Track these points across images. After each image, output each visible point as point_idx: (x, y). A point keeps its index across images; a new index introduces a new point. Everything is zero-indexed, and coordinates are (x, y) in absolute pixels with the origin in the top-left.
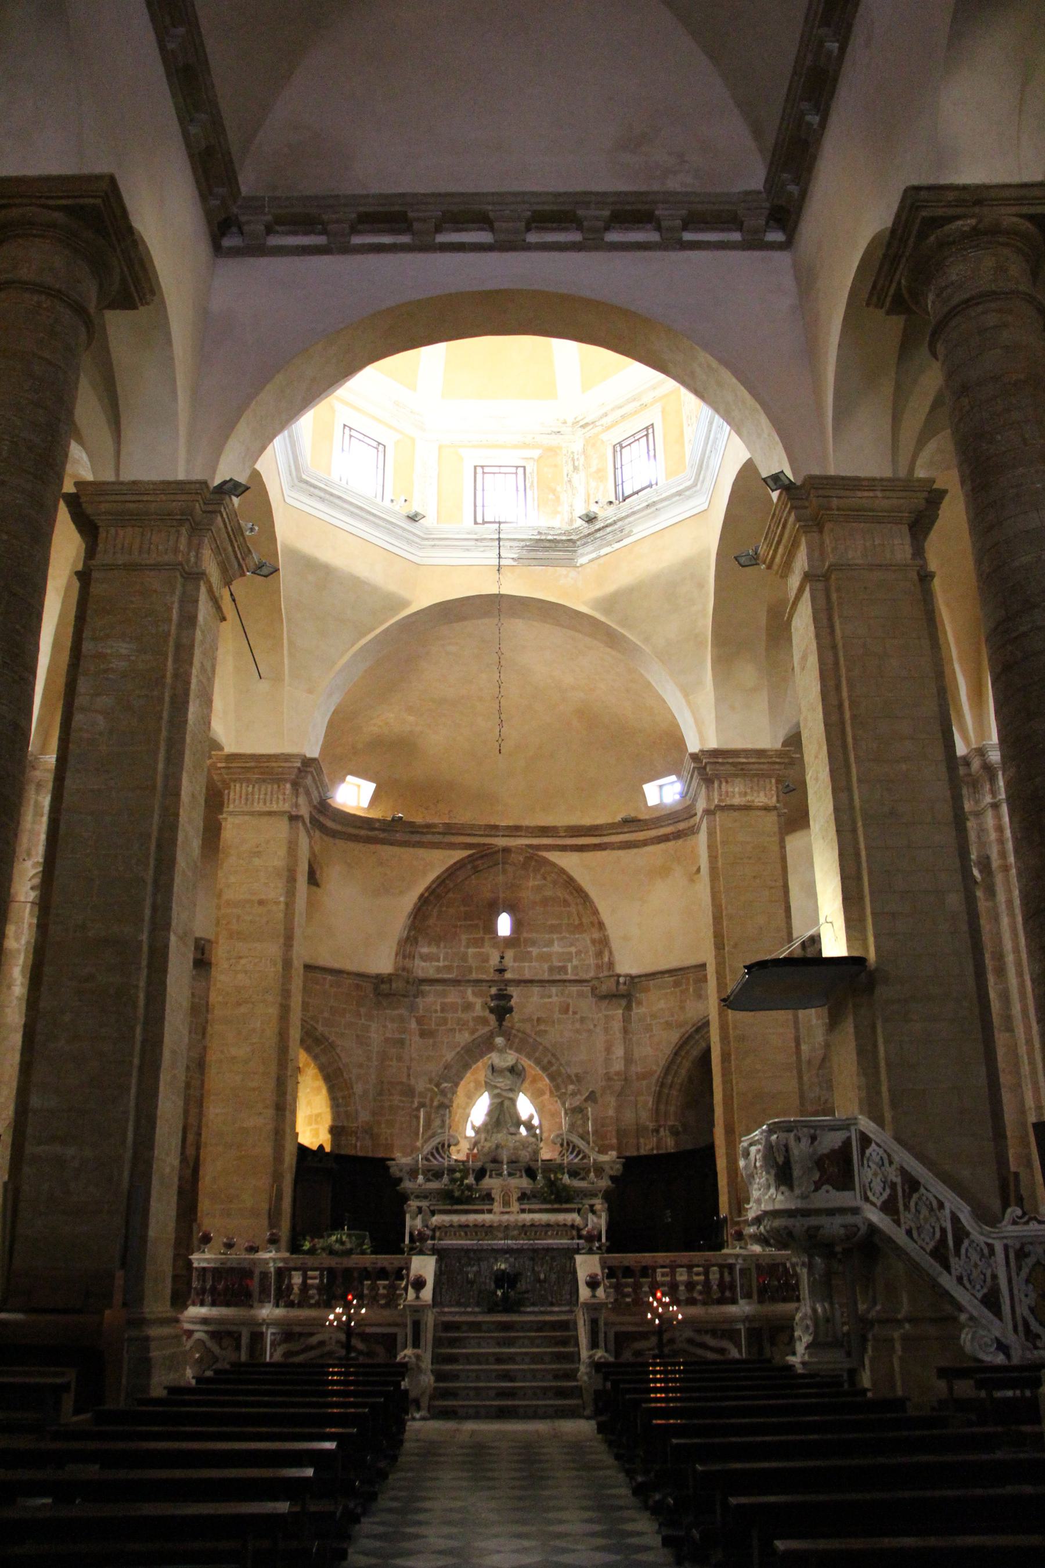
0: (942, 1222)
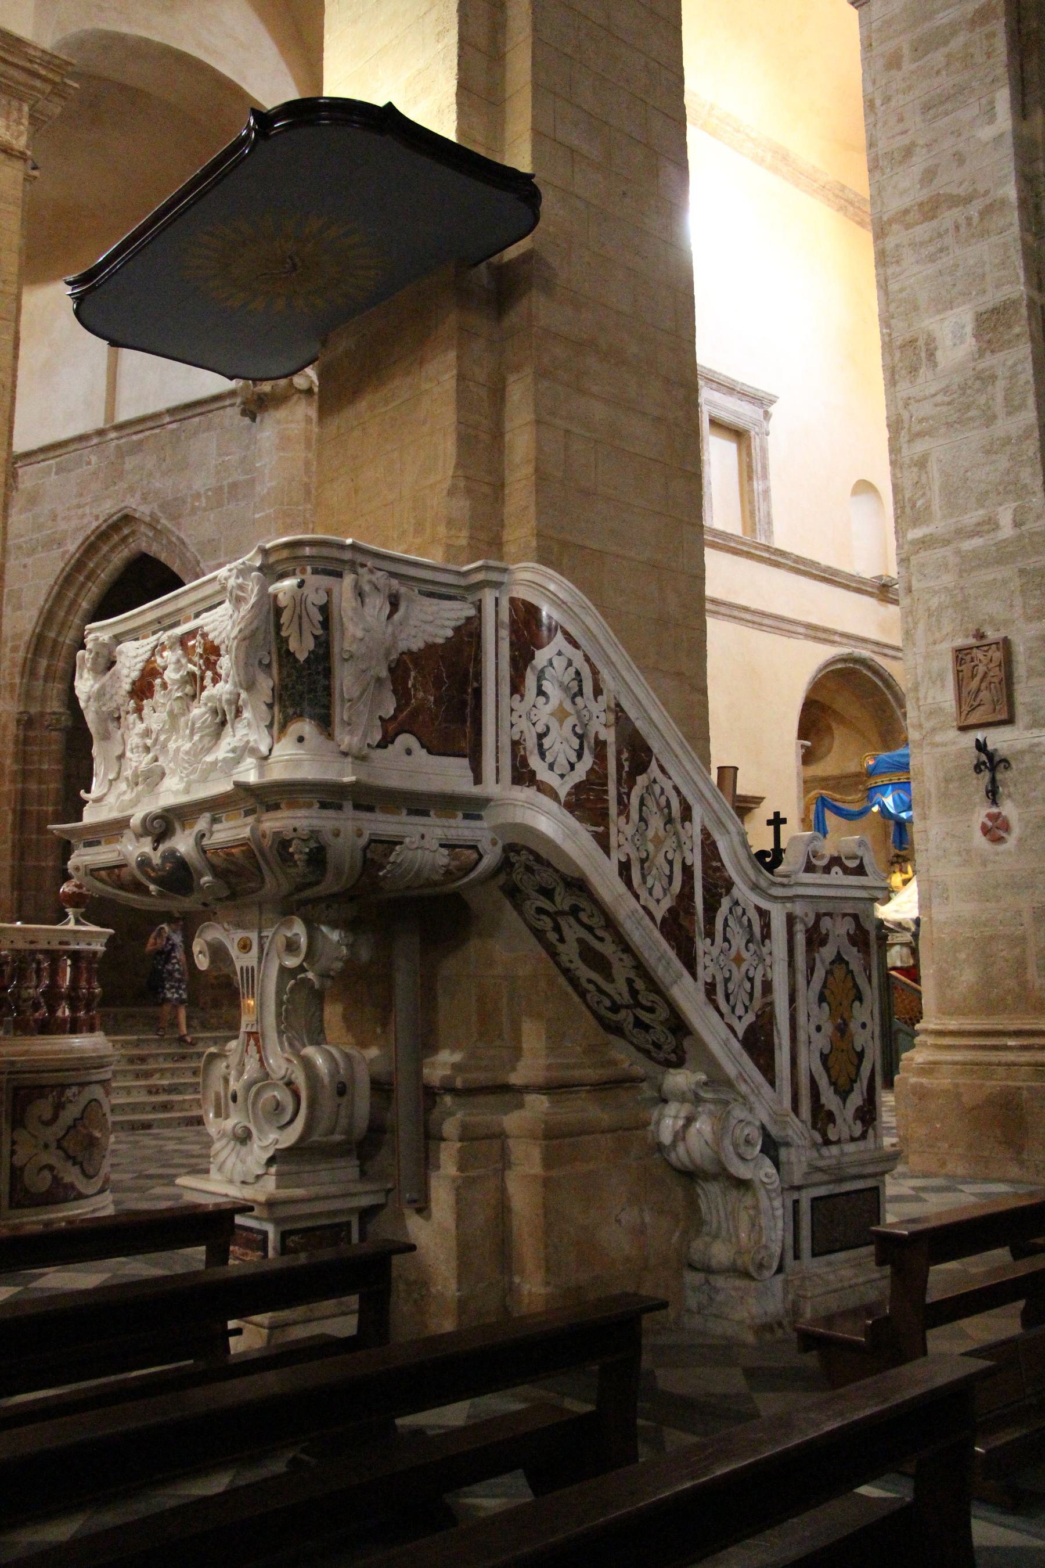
0: (688, 854)
